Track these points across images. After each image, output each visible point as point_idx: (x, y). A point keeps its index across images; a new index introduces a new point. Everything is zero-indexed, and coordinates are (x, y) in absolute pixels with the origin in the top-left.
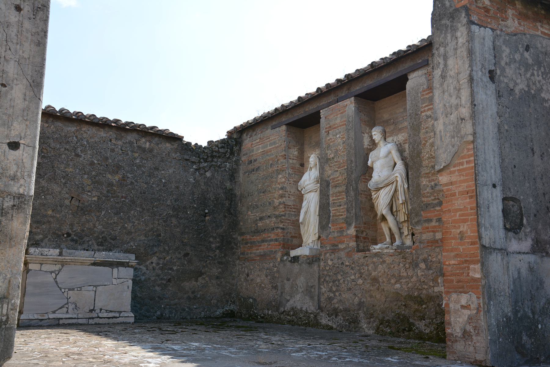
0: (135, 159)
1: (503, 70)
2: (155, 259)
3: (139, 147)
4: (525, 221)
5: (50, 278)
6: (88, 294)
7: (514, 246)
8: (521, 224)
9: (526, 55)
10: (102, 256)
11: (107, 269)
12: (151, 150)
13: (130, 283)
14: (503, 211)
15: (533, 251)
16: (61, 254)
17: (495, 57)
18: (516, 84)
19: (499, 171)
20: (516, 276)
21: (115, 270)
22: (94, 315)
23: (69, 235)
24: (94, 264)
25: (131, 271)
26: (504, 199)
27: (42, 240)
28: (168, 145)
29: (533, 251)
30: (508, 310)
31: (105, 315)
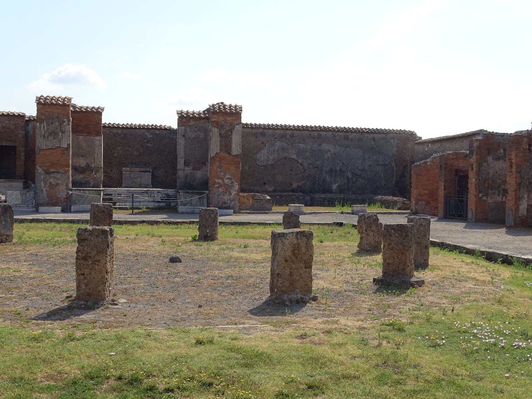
0: (154, 137)
1: (187, 134)
2: (162, 169)
3: (155, 133)
4: (191, 164)
5: (128, 176)
6: (139, 179)
7: (187, 169)
8: (190, 165)
9: (195, 129)
10: (142, 169)
11: (144, 173)
12: (159, 134)
13: (151, 177)
14: (184, 163)
15: (192, 169)
16: (130, 169)
17: (185, 132)
18: (191, 136)
19: (184, 155)
20: (186, 174)
21: (146, 173)
22: (141, 185)
23: (135, 163)
24: (140, 172)
25: (151, 173)
26: (185, 161)
27: (128, 165)
28: (165, 131)
29: (192, 169)
30: (183, 180)
31: (144, 185)
